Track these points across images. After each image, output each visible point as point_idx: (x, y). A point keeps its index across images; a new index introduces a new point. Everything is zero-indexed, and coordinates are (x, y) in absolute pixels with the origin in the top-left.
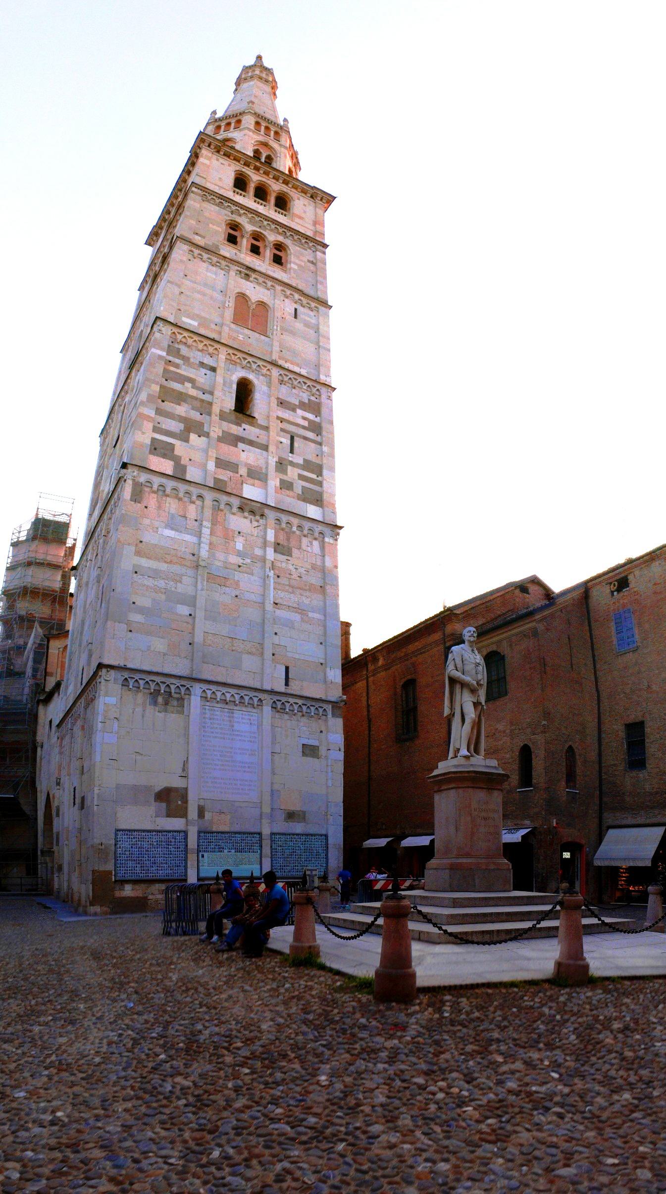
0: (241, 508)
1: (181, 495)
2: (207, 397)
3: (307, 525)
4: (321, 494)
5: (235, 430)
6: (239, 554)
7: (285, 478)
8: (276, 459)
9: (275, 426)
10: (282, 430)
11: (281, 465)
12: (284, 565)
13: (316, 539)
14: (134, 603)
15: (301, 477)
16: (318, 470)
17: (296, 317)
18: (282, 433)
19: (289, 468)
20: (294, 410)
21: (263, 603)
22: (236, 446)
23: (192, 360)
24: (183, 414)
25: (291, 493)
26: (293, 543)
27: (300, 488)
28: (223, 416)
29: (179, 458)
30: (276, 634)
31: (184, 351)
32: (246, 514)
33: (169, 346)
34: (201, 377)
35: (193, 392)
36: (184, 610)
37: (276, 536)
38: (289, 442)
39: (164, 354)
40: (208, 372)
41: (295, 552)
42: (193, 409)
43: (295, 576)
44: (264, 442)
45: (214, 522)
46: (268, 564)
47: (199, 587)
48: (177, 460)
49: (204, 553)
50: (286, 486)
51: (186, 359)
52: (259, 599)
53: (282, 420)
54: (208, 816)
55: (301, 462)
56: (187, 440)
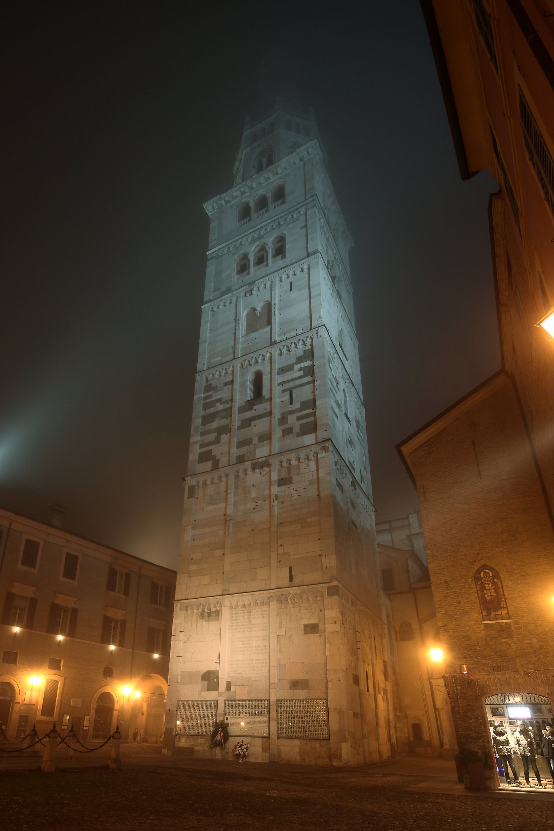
0: (254, 468)
7: (287, 426)
9: (277, 390)
10: (283, 391)
11: (283, 419)
12: (287, 493)
15: (299, 418)
16: (312, 404)
19: (290, 417)
27: (299, 426)
28: (242, 410)
30: (281, 545)
38: (288, 397)
41: (295, 479)
43: (296, 497)
45: (236, 488)
46: (273, 498)
49: (230, 511)
50: (287, 432)
54: (233, 688)
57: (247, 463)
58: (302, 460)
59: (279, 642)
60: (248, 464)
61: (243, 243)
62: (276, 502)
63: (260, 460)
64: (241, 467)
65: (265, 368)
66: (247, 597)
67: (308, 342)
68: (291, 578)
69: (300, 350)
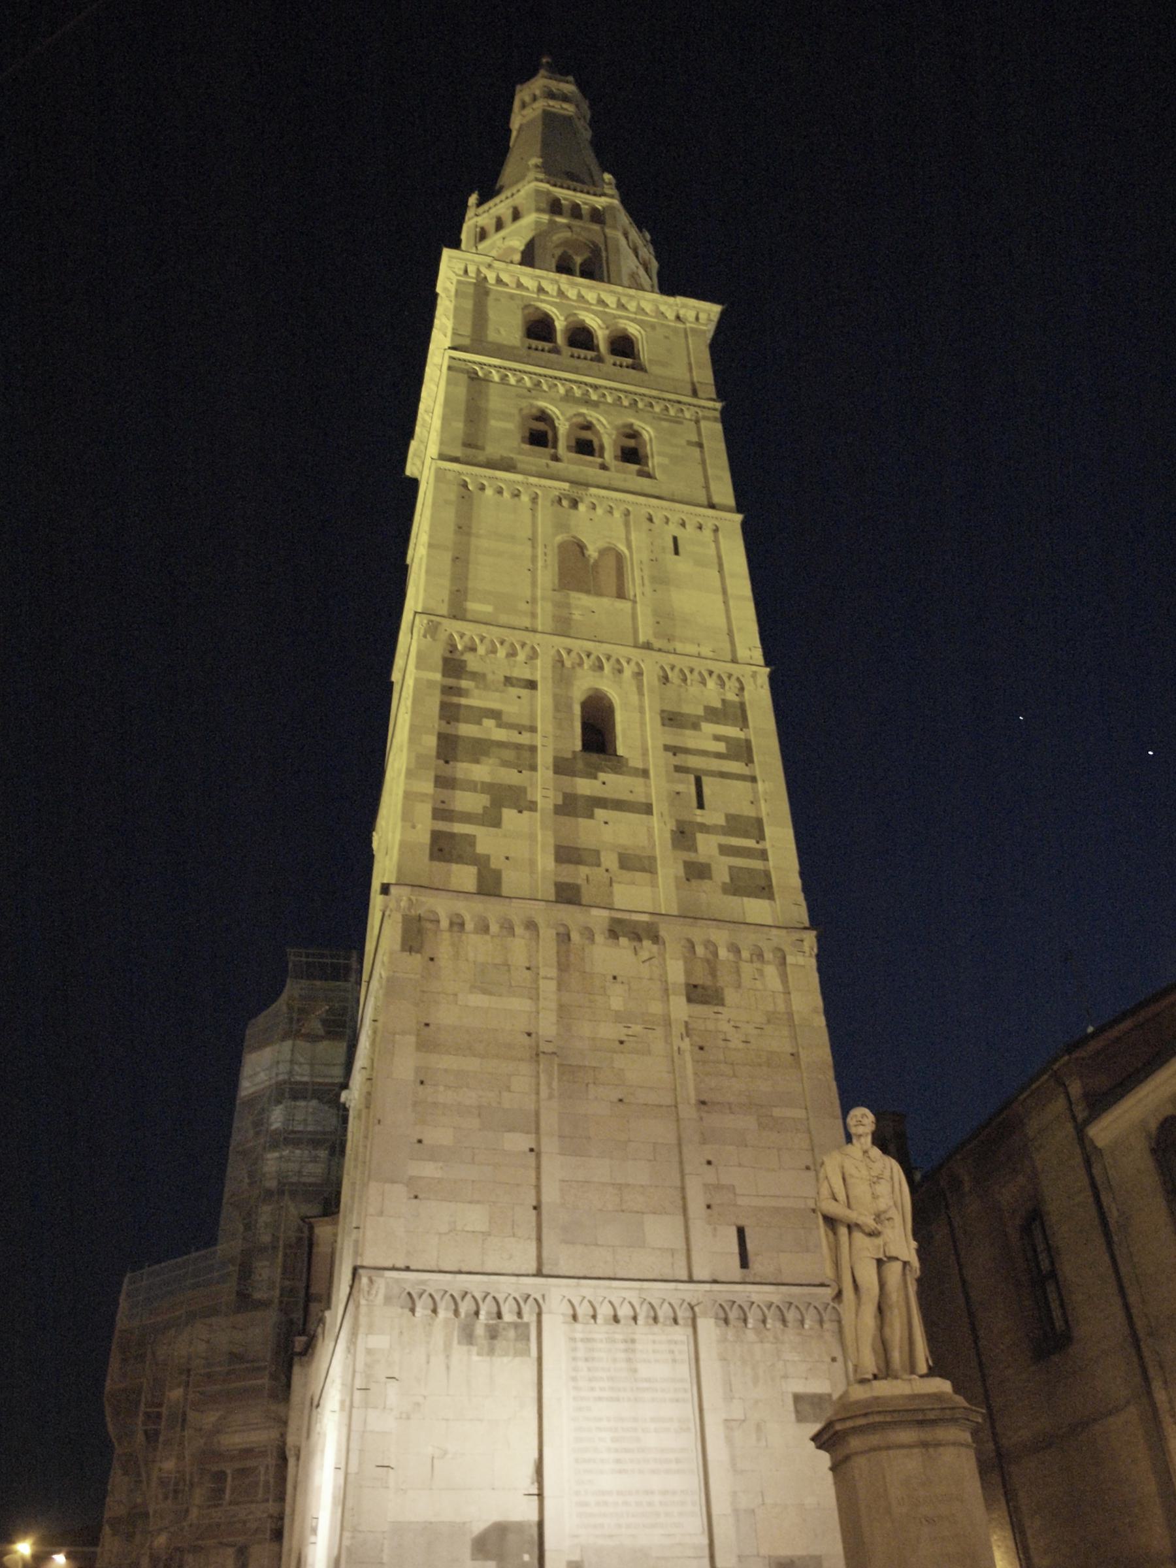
1: (494, 928)
2: (525, 739)
3: (746, 940)
4: (767, 874)
5: (584, 786)
6: (619, 1017)
7: (691, 856)
8: (671, 825)
10: (678, 769)
11: (683, 835)
12: (711, 1026)
13: (769, 963)
14: (420, 1141)
15: (725, 850)
17: (677, 552)
18: (677, 775)
20: (696, 726)
21: (676, 1107)
22: (591, 816)
23: (490, 677)
24: (487, 779)
25: (706, 884)
26: (725, 979)
27: (727, 869)
29: (488, 857)
30: (709, 1163)
31: (472, 662)
32: (623, 941)
33: (446, 661)
34: (511, 704)
35: (500, 735)
36: (520, 1142)
37: (688, 973)
39: (438, 676)
40: (524, 692)
41: (730, 995)
42: (505, 764)
43: (736, 1043)
44: (643, 800)
45: (563, 967)
47: (544, 1093)
48: (481, 863)
49: (548, 1026)
50: (697, 872)
52: (669, 1100)
53: (674, 750)
55: (722, 821)
56: (497, 823)
57: (595, 912)
58: (745, 954)
59: (729, 1440)
60: (599, 917)
62: (687, 1040)
63: (635, 917)
64: (569, 915)
66: (625, 1294)
68: (744, 1263)
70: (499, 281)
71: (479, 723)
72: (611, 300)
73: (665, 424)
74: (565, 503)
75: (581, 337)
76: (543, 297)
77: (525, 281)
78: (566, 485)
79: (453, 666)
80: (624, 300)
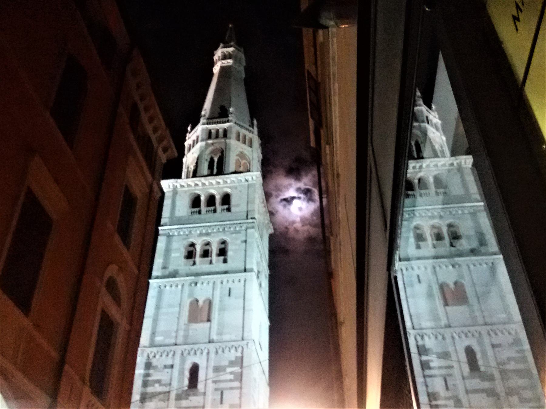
17: (229, 295)
23: (159, 366)
40: (169, 370)
51: (155, 368)
61: (192, 232)
65: (201, 361)
67: (240, 350)
69: (232, 355)
70: (182, 186)
71: (154, 386)
72: (221, 181)
73: (234, 235)
74: (193, 285)
75: (211, 200)
76: (197, 188)
77: (189, 183)
78: (193, 278)
79: (148, 366)
80: (225, 180)
